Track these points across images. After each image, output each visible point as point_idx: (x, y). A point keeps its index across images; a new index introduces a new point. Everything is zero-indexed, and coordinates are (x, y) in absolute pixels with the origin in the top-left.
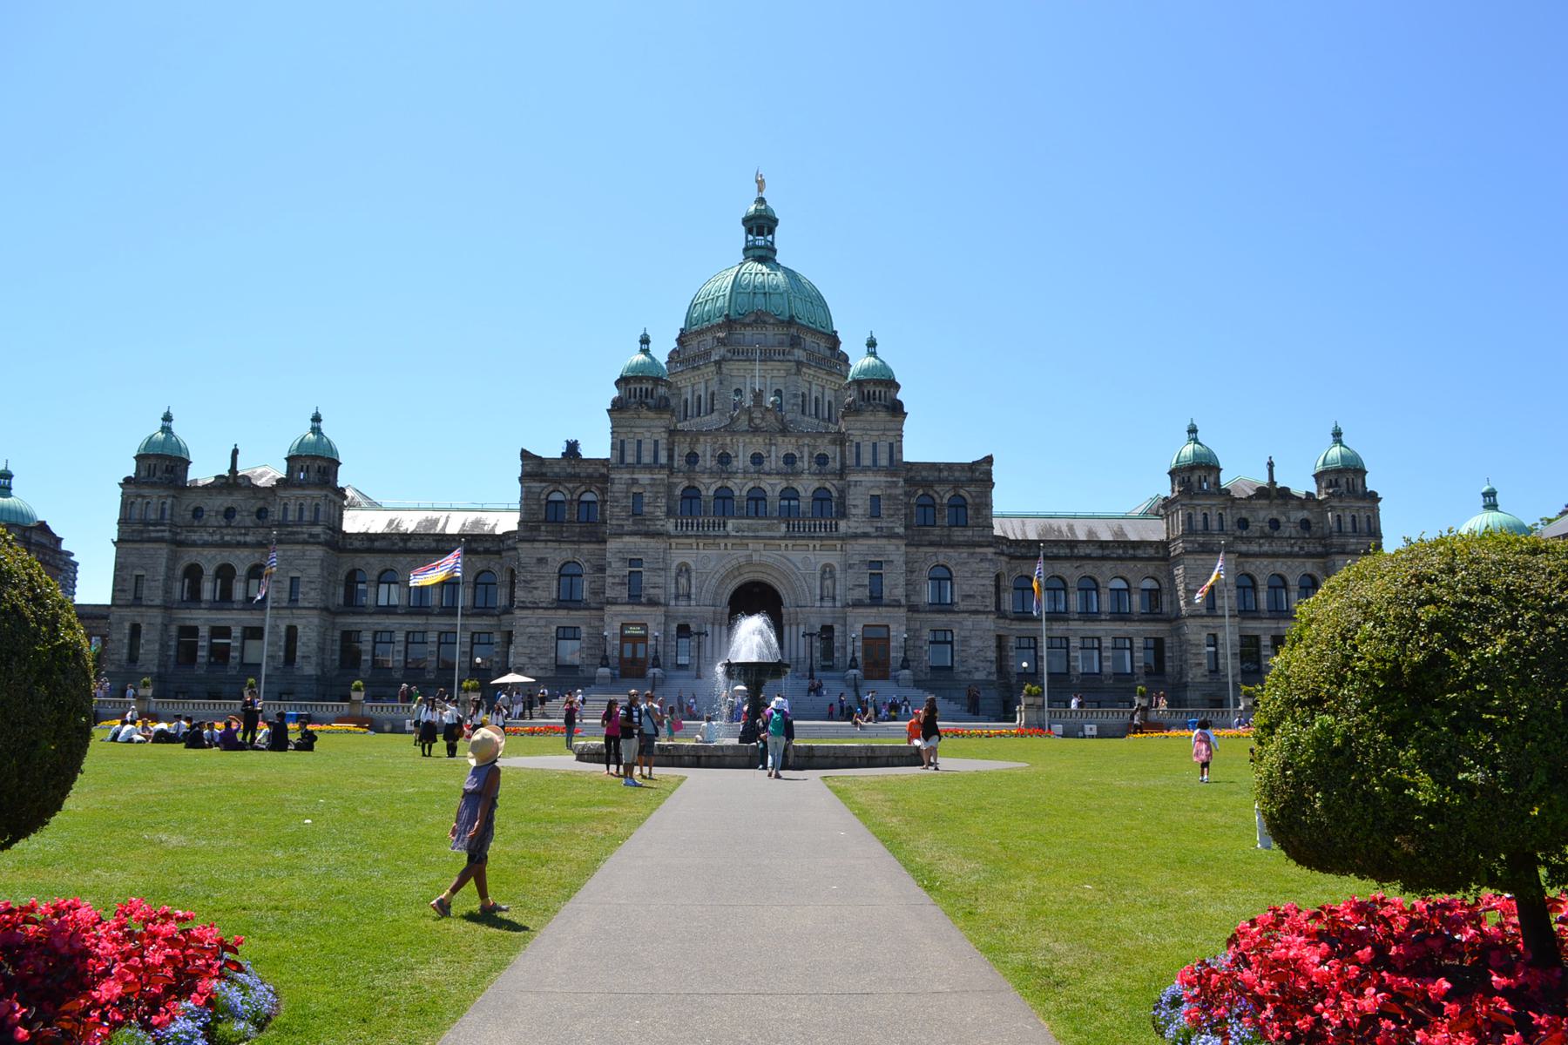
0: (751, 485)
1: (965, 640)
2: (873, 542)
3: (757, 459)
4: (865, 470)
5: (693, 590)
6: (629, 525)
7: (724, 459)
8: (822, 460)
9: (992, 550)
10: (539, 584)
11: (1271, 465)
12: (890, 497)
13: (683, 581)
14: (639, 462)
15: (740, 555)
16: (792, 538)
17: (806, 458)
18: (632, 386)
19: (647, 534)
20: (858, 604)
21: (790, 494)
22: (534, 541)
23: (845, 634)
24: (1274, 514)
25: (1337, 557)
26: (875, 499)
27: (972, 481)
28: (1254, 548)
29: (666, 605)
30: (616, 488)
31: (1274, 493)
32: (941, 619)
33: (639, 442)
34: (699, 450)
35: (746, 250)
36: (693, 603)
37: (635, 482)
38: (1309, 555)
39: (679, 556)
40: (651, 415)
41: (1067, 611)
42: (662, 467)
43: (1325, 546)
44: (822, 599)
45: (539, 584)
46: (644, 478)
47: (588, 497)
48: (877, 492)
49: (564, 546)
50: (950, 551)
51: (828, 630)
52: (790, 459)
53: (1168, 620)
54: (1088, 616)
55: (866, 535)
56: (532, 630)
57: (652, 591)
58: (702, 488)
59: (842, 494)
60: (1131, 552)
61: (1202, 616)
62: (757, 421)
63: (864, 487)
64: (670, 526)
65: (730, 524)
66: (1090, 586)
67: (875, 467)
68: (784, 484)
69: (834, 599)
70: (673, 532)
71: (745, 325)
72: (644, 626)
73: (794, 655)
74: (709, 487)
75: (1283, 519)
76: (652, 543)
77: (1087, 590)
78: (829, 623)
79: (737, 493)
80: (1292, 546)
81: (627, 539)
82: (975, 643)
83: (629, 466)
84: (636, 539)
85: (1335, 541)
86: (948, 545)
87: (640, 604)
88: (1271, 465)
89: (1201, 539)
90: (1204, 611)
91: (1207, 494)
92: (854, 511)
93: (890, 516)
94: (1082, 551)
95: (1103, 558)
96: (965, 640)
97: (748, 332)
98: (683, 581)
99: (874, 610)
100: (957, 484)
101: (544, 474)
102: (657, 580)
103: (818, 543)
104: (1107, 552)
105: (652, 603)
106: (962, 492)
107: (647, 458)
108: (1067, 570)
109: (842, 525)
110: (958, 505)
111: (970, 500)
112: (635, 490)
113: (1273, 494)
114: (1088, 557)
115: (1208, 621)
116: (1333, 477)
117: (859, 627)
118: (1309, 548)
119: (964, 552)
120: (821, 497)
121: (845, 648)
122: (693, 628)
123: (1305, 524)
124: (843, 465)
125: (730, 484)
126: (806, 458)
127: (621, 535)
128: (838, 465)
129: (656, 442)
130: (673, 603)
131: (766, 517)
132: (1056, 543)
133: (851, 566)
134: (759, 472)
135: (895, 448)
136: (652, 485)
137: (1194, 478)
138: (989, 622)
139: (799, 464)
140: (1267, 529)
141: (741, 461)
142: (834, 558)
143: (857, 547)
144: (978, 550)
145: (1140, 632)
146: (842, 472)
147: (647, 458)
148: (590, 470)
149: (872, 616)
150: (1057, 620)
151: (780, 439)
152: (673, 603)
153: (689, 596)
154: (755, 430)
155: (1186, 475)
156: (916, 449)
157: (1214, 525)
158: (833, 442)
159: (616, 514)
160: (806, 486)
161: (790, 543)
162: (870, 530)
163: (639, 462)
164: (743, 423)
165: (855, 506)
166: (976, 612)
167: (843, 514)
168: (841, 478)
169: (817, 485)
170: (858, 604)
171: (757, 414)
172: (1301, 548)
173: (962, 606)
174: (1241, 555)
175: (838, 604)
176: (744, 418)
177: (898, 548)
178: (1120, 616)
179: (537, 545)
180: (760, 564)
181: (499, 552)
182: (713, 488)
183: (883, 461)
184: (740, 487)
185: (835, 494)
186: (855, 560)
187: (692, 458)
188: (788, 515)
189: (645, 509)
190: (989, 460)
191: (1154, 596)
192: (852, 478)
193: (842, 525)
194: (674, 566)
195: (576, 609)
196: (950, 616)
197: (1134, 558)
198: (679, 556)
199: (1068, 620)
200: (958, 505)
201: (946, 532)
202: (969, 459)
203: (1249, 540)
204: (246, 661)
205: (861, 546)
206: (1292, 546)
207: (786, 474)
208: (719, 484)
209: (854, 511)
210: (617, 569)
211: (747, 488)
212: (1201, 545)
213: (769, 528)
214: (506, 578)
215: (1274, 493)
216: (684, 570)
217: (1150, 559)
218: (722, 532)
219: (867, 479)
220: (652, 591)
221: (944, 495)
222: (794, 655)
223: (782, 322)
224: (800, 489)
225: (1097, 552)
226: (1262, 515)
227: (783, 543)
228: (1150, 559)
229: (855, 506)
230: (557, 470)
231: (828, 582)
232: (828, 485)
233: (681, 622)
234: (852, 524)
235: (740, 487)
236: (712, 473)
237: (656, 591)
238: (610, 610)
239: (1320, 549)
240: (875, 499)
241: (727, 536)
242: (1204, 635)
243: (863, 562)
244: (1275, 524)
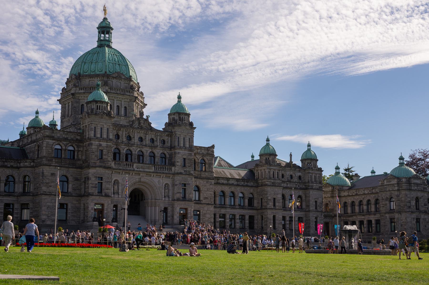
0: (139, 149)
1: (205, 214)
2: (184, 176)
3: (141, 139)
4: (181, 148)
5: (120, 191)
6: (98, 163)
7: (129, 138)
8: (164, 142)
9: (214, 181)
10: (52, 184)
11: (291, 155)
12: (189, 159)
13: (116, 187)
14: (101, 137)
15: (136, 178)
16: (156, 173)
17: (158, 141)
18: (99, 105)
19: (105, 168)
20: (178, 200)
21: (153, 156)
22: (50, 166)
23: (173, 211)
24: (292, 173)
25: (311, 190)
26: (185, 159)
27: (208, 154)
28: (285, 185)
29: (111, 197)
30: (93, 147)
31: (292, 166)
32: (197, 207)
33: (101, 128)
34: (120, 133)
35: (99, 40)
36: (120, 196)
37: (100, 145)
38: (301, 189)
39: (115, 177)
40: (107, 118)
41: (224, 204)
42: (110, 140)
43: (305, 186)
44: (165, 197)
45: (52, 184)
46: (104, 144)
47: (71, 148)
48: (185, 157)
49: (62, 168)
50: (201, 181)
51: (165, 210)
52: (152, 140)
53: (257, 210)
54: (233, 207)
55: (181, 173)
56: (49, 204)
57: (107, 191)
58: (121, 149)
59: (172, 156)
60: (246, 183)
61: (272, 209)
62: (142, 124)
63: (181, 155)
64: (113, 165)
65: (135, 166)
66: (233, 195)
67: (184, 147)
68: (150, 150)
69: (169, 198)
70: (114, 167)
71: (113, 78)
72: (102, 205)
73: (153, 219)
74: (124, 150)
75: (294, 175)
76: (107, 171)
77: (63, 181)
78: (167, 206)
79: (134, 153)
80: (296, 185)
81: (98, 169)
82: (208, 216)
83: (97, 138)
84: (101, 169)
85: (310, 184)
86: (200, 178)
87: (102, 196)
88: (291, 155)
89: (272, 181)
90: (273, 207)
91: (275, 166)
92: (178, 164)
93: (189, 166)
94: (231, 182)
95: (238, 185)
96: (205, 214)
97: (114, 81)
98: (116, 187)
99: (184, 202)
100: (203, 155)
101: (53, 137)
102: (108, 186)
103: (164, 175)
104: (239, 183)
105: (107, 196)
106: (205, 158)
107: (105, 136)
108: (227, 189)
109: (173, 168)
110: (204, 162)
111: (207, 161)
112: (100, 148)
113: (290, 165)
114: (232, 184)
115: (274, 211)
116: (309, 161)
117: (178, 209)
118: (301, 186)
119: (206, 180)
120: (163, 157)
121: (173, 217)
122: (119, 205)
123: (300, 177)
124: (171, 145)
125: (131, 149)
126: (158, 141)
127: (95, 167)
128: (169, 145)
129: (108, 129)
130: (112, 196)
131: (143, 163)
132: (223, 178)
133: (176, 185)
134: (142, 145)
135: (191, 140)
136: (107, 147)
137: (271, 159)
138: (212, 208)
139: (155, 143)
140: (289, 178)
141: (136, 140)
142: (169, 181)
143: (178, 178)
144: (210, 181)
145: (247, 213)
146: (172, 148)
147: (105, 136)
148: (72, 137)
149: (183, 204)
150: (223, 207)
151: (150, 133)
152: (112, 196)
153: (118, 193)
154: (142, 128)
155: (267, 157)
156: (199, 141)
157: (276, 176)
158: (168, 135)
159: (94, 158)
160: (158, 152)
161: (155, 174)
162: (182, 171)
163: (101, 137)
164: (136, 125)
165: (178, 162)
166: (208, 204)
167: (173, 164)
168: (171, 150)
169: (162, 152)
170: (178, 200)
171: (142, 121)
172: (299, 186)
173: (204, 201)
174: (284, 188)
175: (170, 199)
176: (137, 123)
177: (192, 179)
178: (242, 207)
179: (51, 167)
180: (143, 182)
181: (18, 168)
182: (125, 149)
183: (187, 146)
184: (135, 151)
185: (168, 156)
186: (177, 183)
187: (118, 136)
188: (153, 163)
189: (104, 157)
190: (213, 147)
191: (251, 201)
192: (177, 151)
193: (173, 168)
194: (113, 181)
195: (68, 196)
196: (200, 205)
197: (247, 186)
198: (115, 177)
199: (226, 208)
200: (204, 162)
201: (199, 173)
202: (207, 146)
203: (284, 182)
204: (23, 219)
205: (179, 179)
206: (296, 185)
207: (152, 146)
208: (127, 148)
209: (178, 164)
210: (93, 181)
211: (137, 151)
212: (273, 183)
213: (148, 169)
214: (21, 180)
215: (292, 166)
216: (116, 182)
217: (252, 186)
218: (132, 169)
219: (182, 152)
220: (107, 191)
221: (199, 158)
222: (153, 219)
223: (127, 78)
224: (156, 153)
225: (236, 183)
226: (288, 173)
227: (152, 174)
228: (252, 186)
229: (178, 162)
230: (59, 135)
231: (167, 190)
232: (165, 152)
233: (115, 204)
234: (176, 168)
235: (135, 151)
236: (125, 145)
237: (108, 191)
238: (91, 198)
239: (304, 187)
240: (185, 159)
241: (134, 170)
242: (272, 215)
243: (180, 184)
244: (291, 177)
